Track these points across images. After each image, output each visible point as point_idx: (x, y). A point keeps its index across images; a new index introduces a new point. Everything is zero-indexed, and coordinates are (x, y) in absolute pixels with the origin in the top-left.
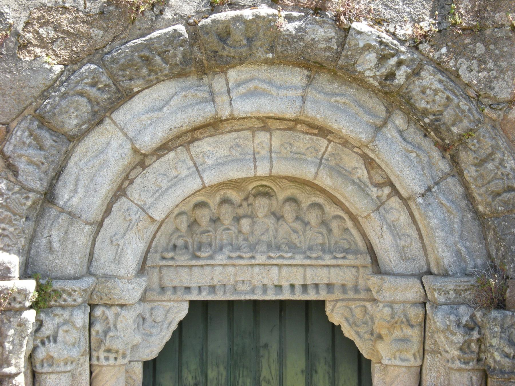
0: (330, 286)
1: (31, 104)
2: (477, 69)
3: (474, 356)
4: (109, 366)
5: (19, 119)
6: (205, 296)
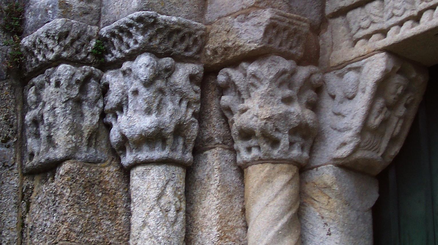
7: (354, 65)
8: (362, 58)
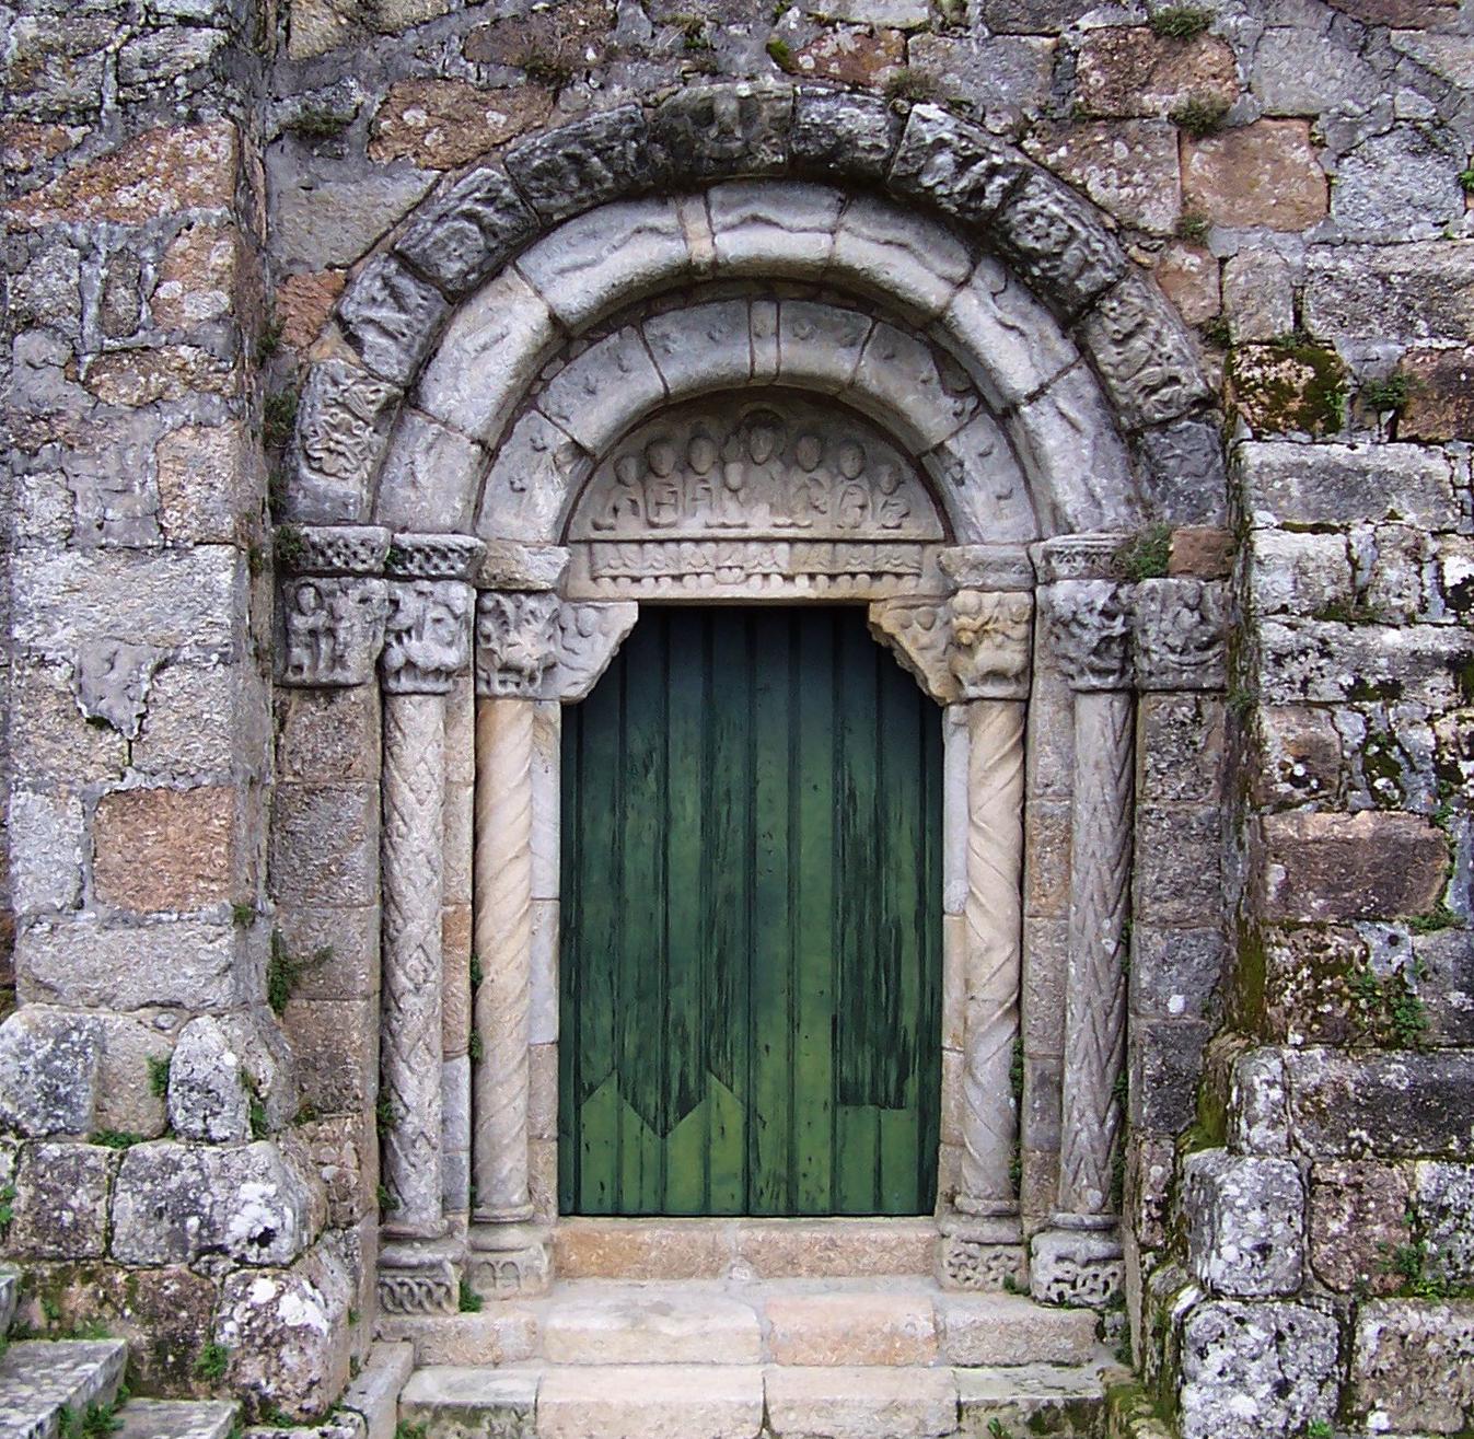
0: (876, 575)
1: (385, 234)
2: (1116, 182)
3: (1115, 664)
4: (507, 696)
5: (367, 259)
6: (668, 591)
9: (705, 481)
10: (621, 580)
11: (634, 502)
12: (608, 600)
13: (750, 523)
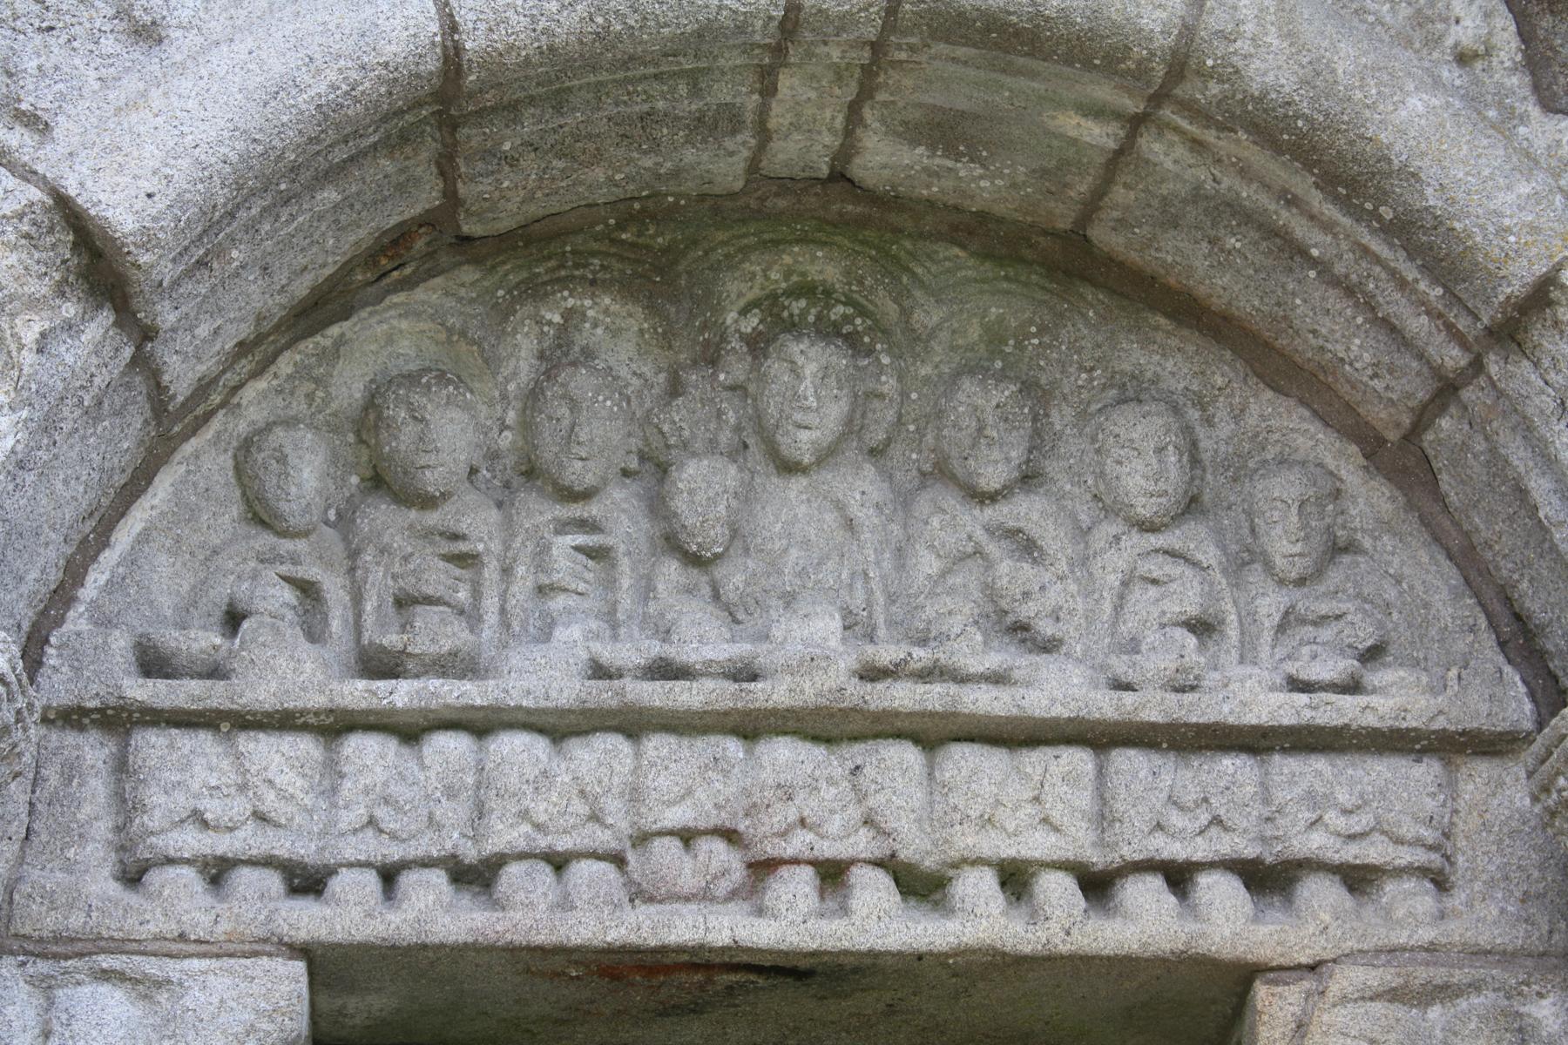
7: (152, 966)
8: (192, 948)
9: (585, 525)
10: (245, 879)
11: (307, 590)
12: (182, 944)
13: (763, 655)
